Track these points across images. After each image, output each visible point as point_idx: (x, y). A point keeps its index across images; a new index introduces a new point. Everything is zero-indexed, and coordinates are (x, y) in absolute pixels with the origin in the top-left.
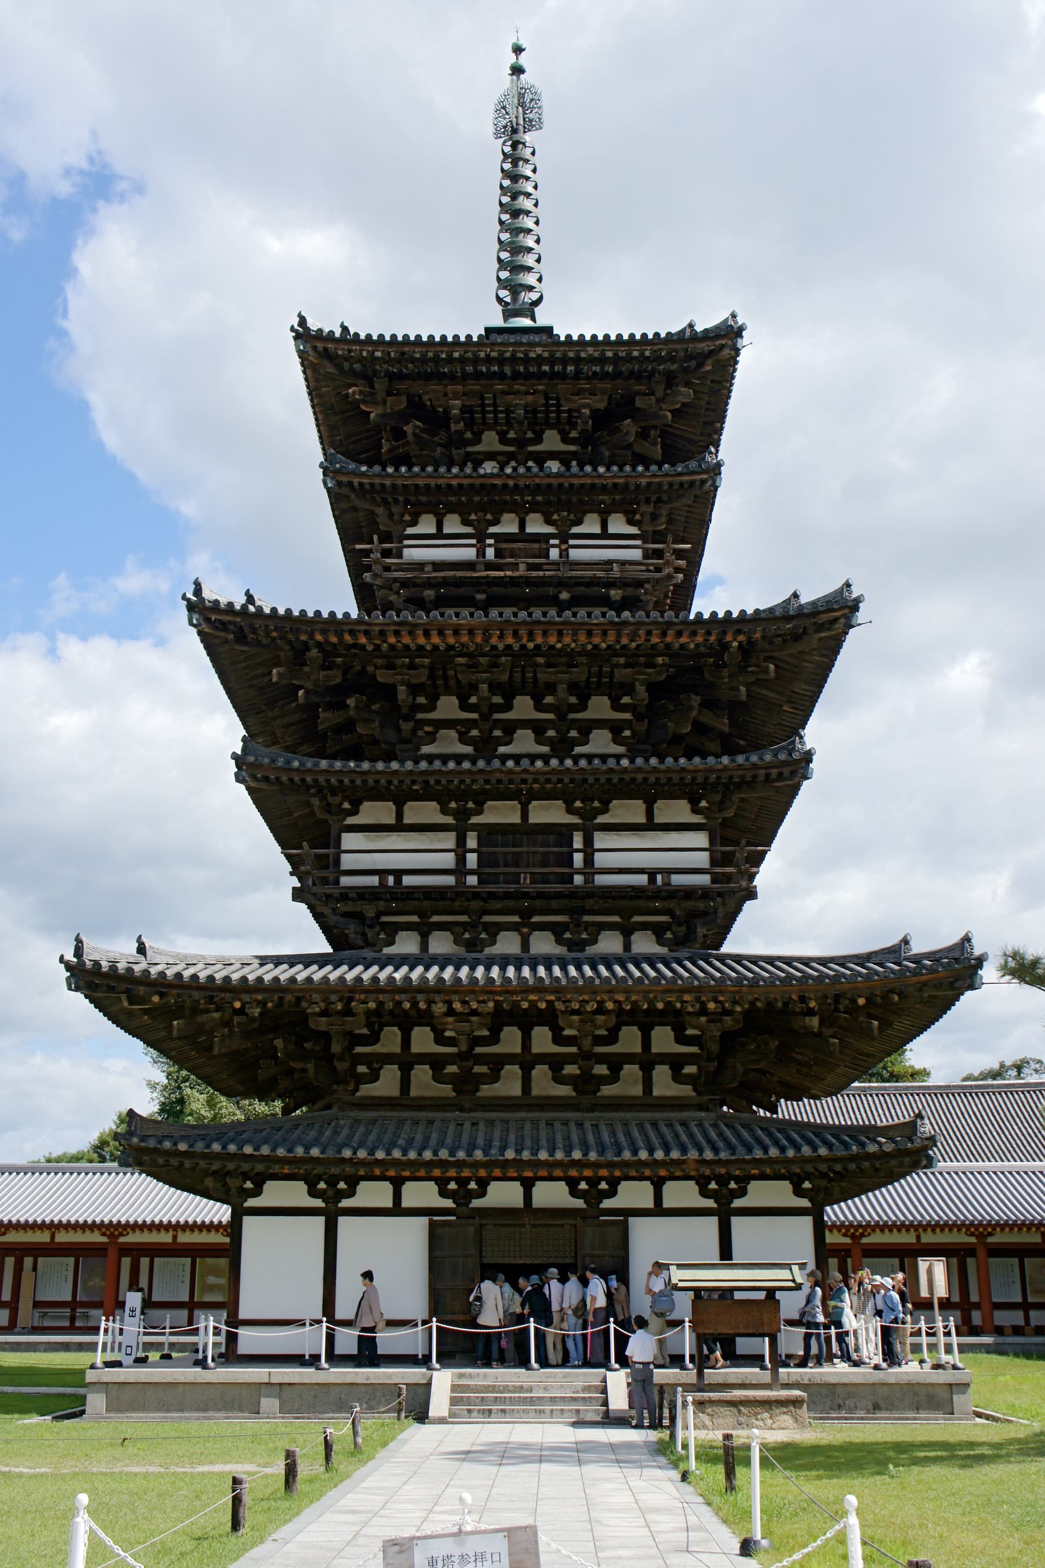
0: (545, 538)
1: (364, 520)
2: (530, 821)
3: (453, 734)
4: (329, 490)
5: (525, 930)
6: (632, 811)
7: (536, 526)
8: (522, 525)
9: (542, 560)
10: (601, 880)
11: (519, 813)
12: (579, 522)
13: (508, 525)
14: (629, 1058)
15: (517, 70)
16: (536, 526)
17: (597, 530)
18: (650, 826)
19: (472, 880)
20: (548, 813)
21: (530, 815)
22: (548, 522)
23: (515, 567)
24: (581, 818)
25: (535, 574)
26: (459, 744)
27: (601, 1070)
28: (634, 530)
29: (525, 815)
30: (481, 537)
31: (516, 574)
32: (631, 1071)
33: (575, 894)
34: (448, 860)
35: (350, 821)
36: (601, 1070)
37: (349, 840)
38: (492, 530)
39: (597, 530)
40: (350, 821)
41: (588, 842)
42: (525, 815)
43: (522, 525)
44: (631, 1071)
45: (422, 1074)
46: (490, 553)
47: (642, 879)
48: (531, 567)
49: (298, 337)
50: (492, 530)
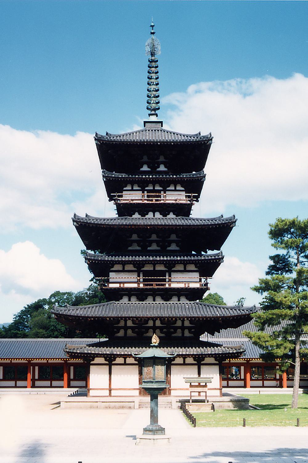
0: (159, 191)
1: (113, 188)
2: (156, 269)
3: (136, 244)
4: (104, 181)
5: (154, 296)
7: (158, 188)
8: (154, 188)
9: (159, 198)
11: (153, 267)
12: (169, 187)
14: (179, 327)
16: (158, 188)
17: (174, 189)
21: (156, 268)
22: (160, 186)
23: (152, 200)
24: (168, 268)
25: (157, 202)
26: (138, 247)
27: (172, 330)
28: (183, 189)
29: (154, 268)
31: (153, 202)
32: (179, 331)
33: (167, 288)
35: (112, 269)
36: (172, 330)
37: (112, 275)
38: (146, 188)
39: (174, 189)
40: (112, 269)
42: (154, 268)
43: (154, 188)
44: (179, 331)
45: (129, 332)
48: (156, 200)
49: (95, 140)
50: (146, 188)
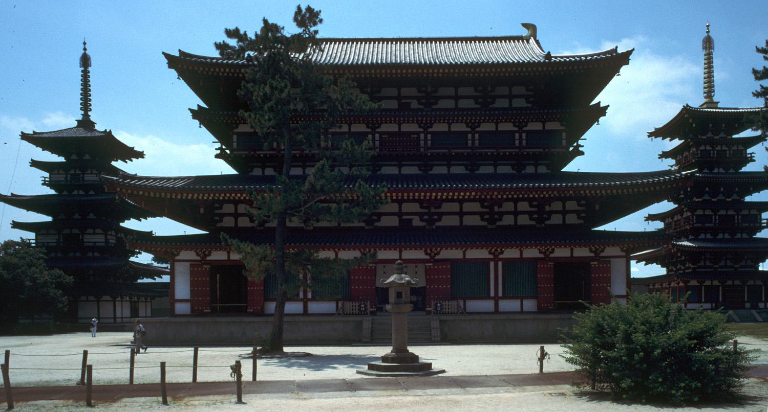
6: (91, 231)
10: (85, 244)
13: (72, 172)
15: (85, 49)
18: (94, 233)
19: (61, 244)
20: (76, 231)
30: (66, 174)
34: (55, 241)
41: (83, 237)
46: (69, 179)
47: (92, 244)
